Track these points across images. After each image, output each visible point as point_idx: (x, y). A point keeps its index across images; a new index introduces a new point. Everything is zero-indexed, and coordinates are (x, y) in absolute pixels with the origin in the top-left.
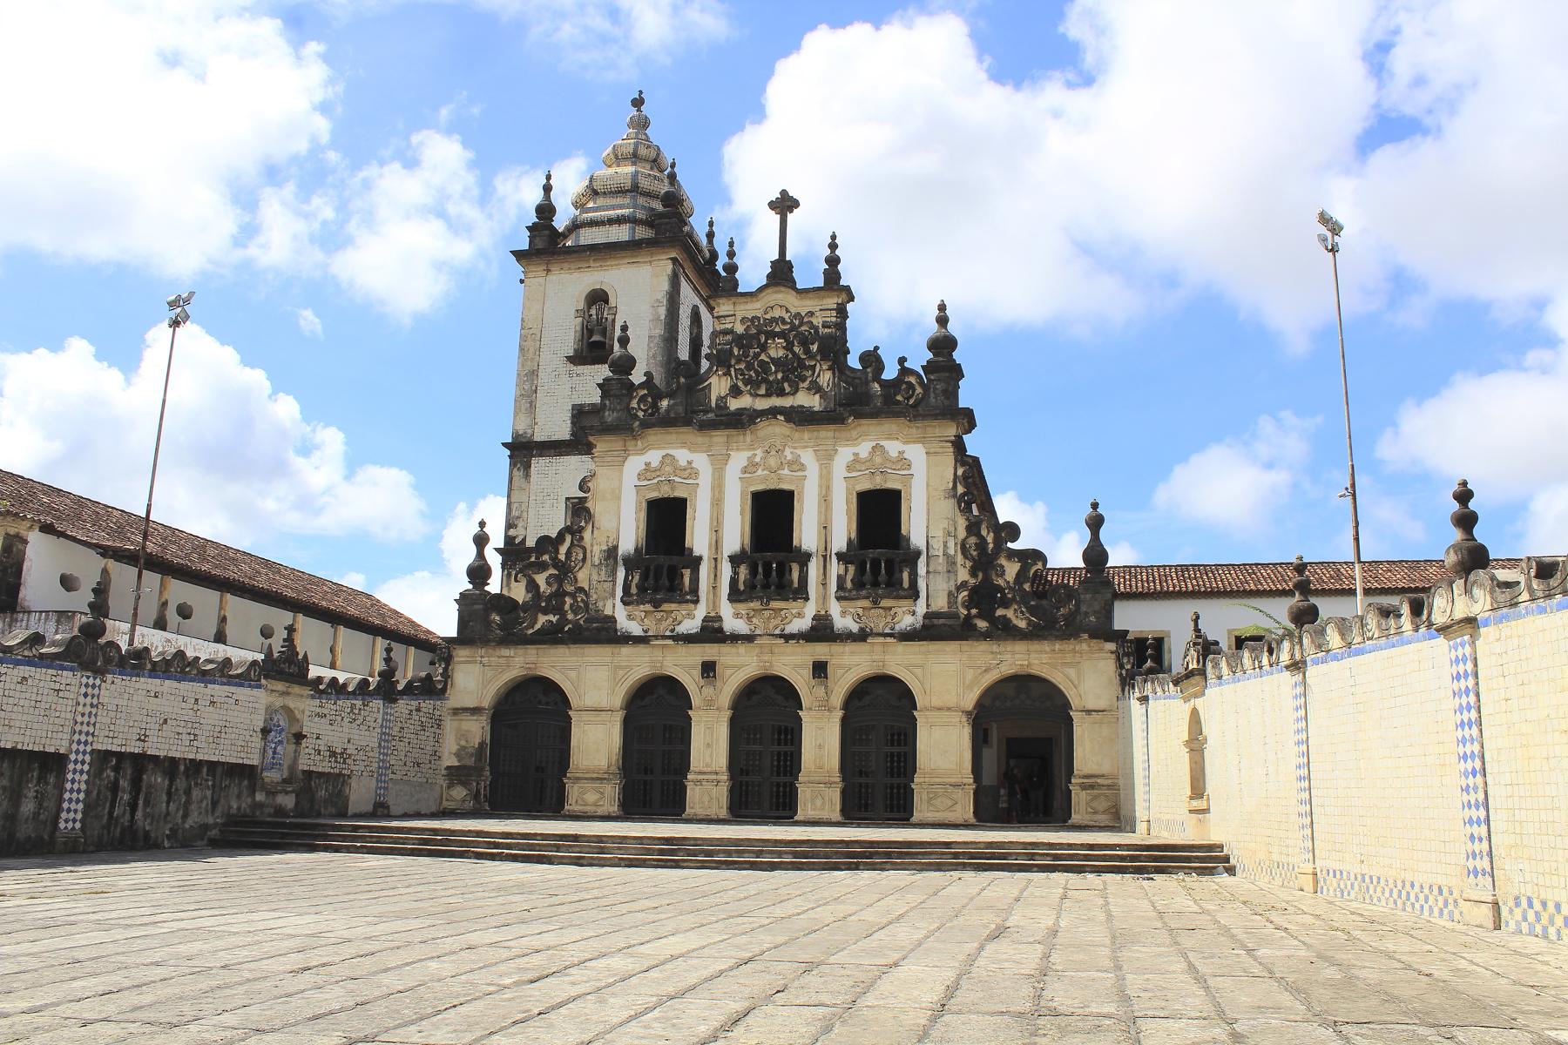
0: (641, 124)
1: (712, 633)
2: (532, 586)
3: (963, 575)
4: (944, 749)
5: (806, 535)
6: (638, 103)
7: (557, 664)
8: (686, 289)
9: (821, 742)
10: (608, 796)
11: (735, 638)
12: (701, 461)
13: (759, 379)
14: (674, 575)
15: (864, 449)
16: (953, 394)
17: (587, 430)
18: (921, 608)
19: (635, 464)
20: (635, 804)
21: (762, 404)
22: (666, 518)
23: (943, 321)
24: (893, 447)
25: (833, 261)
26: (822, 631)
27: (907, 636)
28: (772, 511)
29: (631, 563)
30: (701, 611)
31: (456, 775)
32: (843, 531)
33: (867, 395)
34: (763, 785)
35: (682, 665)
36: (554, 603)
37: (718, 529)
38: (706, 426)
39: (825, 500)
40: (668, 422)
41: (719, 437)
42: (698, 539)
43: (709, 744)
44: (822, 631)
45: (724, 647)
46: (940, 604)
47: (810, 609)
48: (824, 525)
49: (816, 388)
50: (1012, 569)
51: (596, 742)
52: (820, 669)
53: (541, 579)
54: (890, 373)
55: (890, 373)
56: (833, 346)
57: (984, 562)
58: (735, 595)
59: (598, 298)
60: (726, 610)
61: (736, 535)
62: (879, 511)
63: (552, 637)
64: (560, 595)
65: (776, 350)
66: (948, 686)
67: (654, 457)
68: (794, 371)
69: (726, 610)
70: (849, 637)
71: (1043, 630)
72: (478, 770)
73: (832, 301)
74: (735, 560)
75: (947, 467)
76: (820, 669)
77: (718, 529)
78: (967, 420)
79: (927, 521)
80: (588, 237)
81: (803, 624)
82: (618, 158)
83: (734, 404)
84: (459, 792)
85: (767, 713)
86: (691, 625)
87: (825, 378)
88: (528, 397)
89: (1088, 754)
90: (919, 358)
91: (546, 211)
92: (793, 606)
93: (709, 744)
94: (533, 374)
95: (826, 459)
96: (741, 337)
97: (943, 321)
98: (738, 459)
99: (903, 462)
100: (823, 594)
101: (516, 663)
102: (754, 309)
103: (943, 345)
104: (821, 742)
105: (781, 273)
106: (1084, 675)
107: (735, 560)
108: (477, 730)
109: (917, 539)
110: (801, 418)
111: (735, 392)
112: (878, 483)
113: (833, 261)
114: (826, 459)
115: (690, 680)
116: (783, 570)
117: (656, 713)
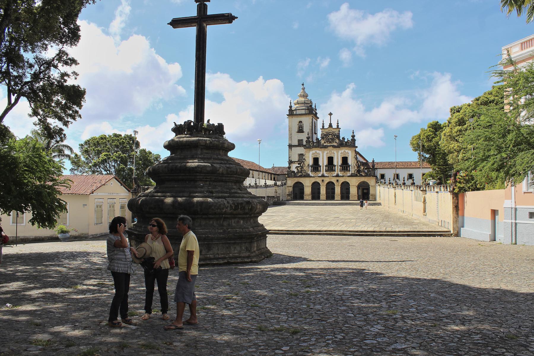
0: (304, 89)
1: (323, 176)
2: (298, 169)
3: (356, 168)
4: (353, 191)
5: (335, 163)
6: (303, 85)
7: (301, 180)
8: (314, 119)
9: (338, 190)
10: (310, 197)
11: (326, 177)
12: (320, 152)
13: (328, 141)
14: (318, 168)
15: (343, 151)
16: (354, 144)
17: (300, 144)
18: (351, 173)
19: (311, 152)
20: (313, 198)
21: (329, 145)
22: (316, 160)
23: (353, 133)
24: (347, 151)
25: (338, 123)
26: (337, 176)
27: (348, 176)
28: (330, 160)
29: (311, 166)
30: (321, 173)
31: (288, 195)
32: (340, 162)
33: (342, 144)
34: (330, 196)
35: (319, 180)
36: (301, 172)
37: (323, 162)
38: (321, 148)
39: (338, 158)
40: (316, 147)
41: (323, 149)
42: (320, 163)
43: (323, 191)
44: (337, 176)
45: (324, 177)
46: (353, 172)
47: (336, 173)
48: (338, 161)
49: (336, 142)
50: (362, 168)
51: (308, 190)
52: (337, 181)
53: (299, 168)
54: (346, 140)
55: (346, 140)
56: (338, 137)
57: (359, 167)
58: (326, 171)
59: (300, 122)
60: (325, 173)
61: (326, 163)
62: (345, 160)
63: (301, 176)
64: (302, 171)
65: (330, 137)
66: (354, 182)
67: (314, 152)
68: (333, 140)
69: (325, 173)
70: (341, 176)
71: (367, 175)
72: (291, 194)
73: (338, 130)
74: (326, 166)
75: (354, 154)
76: (337, 181)
77: (323, 162)
78: (357, 147)
79: (351, 161)
80: (299, 112)
81: (335, 175)
82: (301, 96)
83: (325, 144)
84: (289, 197)
85: (330, 186)
86: (320, 175)
87: (337, 141)
88: (291, 138)
89: (371, 191)
90: (350, 138)
91: (291, 107)
92: (334, 172)
93: (323, 191)
94: (291, 134)
95: (338, 152)
96: (325, 135)
97: (353, 133)
98: (326, 152)
99: (348, 153)
100: (338, 170)
101: (296, 180)
102: (327, 131)
103: (353, 136)
104: (338, 190)
105: (331, 125)
106: (371, 181)
107: (326, 166)
108: (291, 189)
109: (350, 164)
110: (334, 147)
111: (325, 143)
112: (345, 156)
113: (338, 123)
114: (338, 152)
115: (320, 182)
116: (332, 168)
117: (316, 187)
